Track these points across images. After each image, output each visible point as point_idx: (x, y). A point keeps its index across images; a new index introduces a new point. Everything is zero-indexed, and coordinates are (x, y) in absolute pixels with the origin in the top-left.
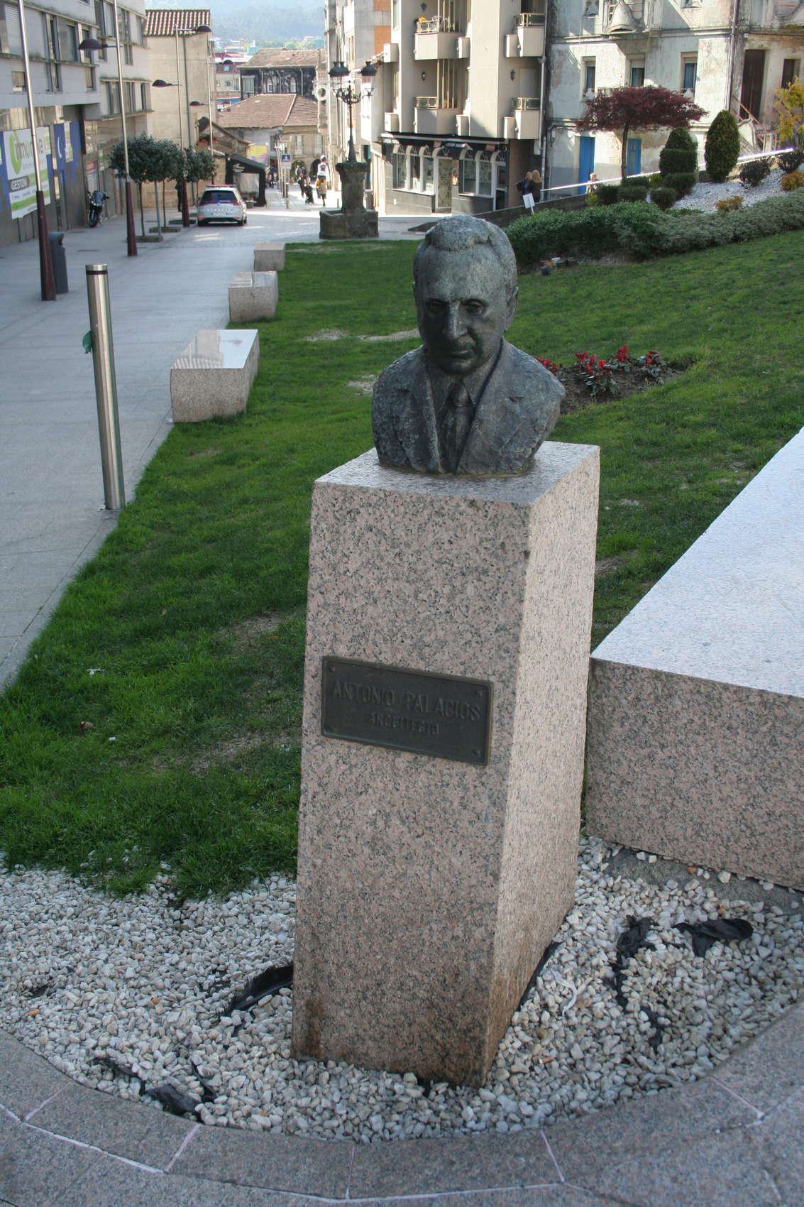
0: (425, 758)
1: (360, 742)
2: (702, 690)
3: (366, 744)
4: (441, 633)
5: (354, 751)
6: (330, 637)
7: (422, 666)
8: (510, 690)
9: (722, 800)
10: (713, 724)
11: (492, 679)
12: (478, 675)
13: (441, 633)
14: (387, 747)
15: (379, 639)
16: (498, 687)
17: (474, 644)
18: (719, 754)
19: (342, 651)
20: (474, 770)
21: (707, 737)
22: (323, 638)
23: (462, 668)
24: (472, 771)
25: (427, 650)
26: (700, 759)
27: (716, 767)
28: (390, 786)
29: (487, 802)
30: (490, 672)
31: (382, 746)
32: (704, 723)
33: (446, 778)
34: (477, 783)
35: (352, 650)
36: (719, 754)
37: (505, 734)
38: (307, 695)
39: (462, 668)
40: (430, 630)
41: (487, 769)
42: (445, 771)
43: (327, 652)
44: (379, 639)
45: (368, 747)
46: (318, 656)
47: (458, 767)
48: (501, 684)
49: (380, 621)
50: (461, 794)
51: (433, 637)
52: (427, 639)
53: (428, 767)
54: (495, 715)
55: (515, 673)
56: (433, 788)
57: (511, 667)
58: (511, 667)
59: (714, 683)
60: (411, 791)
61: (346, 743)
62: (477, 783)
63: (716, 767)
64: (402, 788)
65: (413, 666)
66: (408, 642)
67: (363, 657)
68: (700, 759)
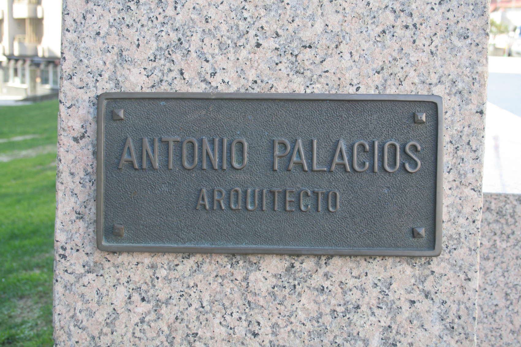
0: (309, 264)
1: (175, 251)
2: (493, 206)
3: (189, 253)
4: (334, 20)
5: (162, 273)
6: (111, 57)
7: (298, 87)
8: (473, 108)
9: (513, 332)
10: (504, 245)
11: (438, 90)
12: (410, 88)
13: (334, 20)
14: (232, 254)
15: (211, 47)
16: (449, 106)
17: (399, 31)
18: (511, 279)
19: (136, 81)
20: (408, 270)
21: (497, 261)
22: (96, 62)
23: (378, 79)
24: (401, 274)
25: (308, 54)
26: (489, 288)
27: (507, 294)
28: (241, 330)
29: (437, 328)
30: (434, 79)
31: (219, 252)
32: (494, 245)
33: (354, 296)
34: (416, 295)
35: (156, 77)
36: (511, 279)
37: (467, 191)
38: (65, 176)
39: (378, 79)
40: (312, 17)
41: (435, 265)
42: (351, 282)
43: (106, 86)
44: (211, 47)
45: (191, 262)
46: (86, 97)
47: (376, 270)
48: (456, 100)
49: (212, 12)
50: (386, 321)
51: (319, 26)
52: (307, 35)
53: (317, 280)
54: (446, 158)
55: (482, 75)
56: (326, 319)
57: (473, 65)
58: (473, 65)
59: (506, 196)
60: (283, 333)
61: (147, 260)
62: (416, 295)
63: (507, 294)
64: (265, 330)
65: (282, 88)
66: (269, 44)
67: (180, 87)
68: (489, 288)
